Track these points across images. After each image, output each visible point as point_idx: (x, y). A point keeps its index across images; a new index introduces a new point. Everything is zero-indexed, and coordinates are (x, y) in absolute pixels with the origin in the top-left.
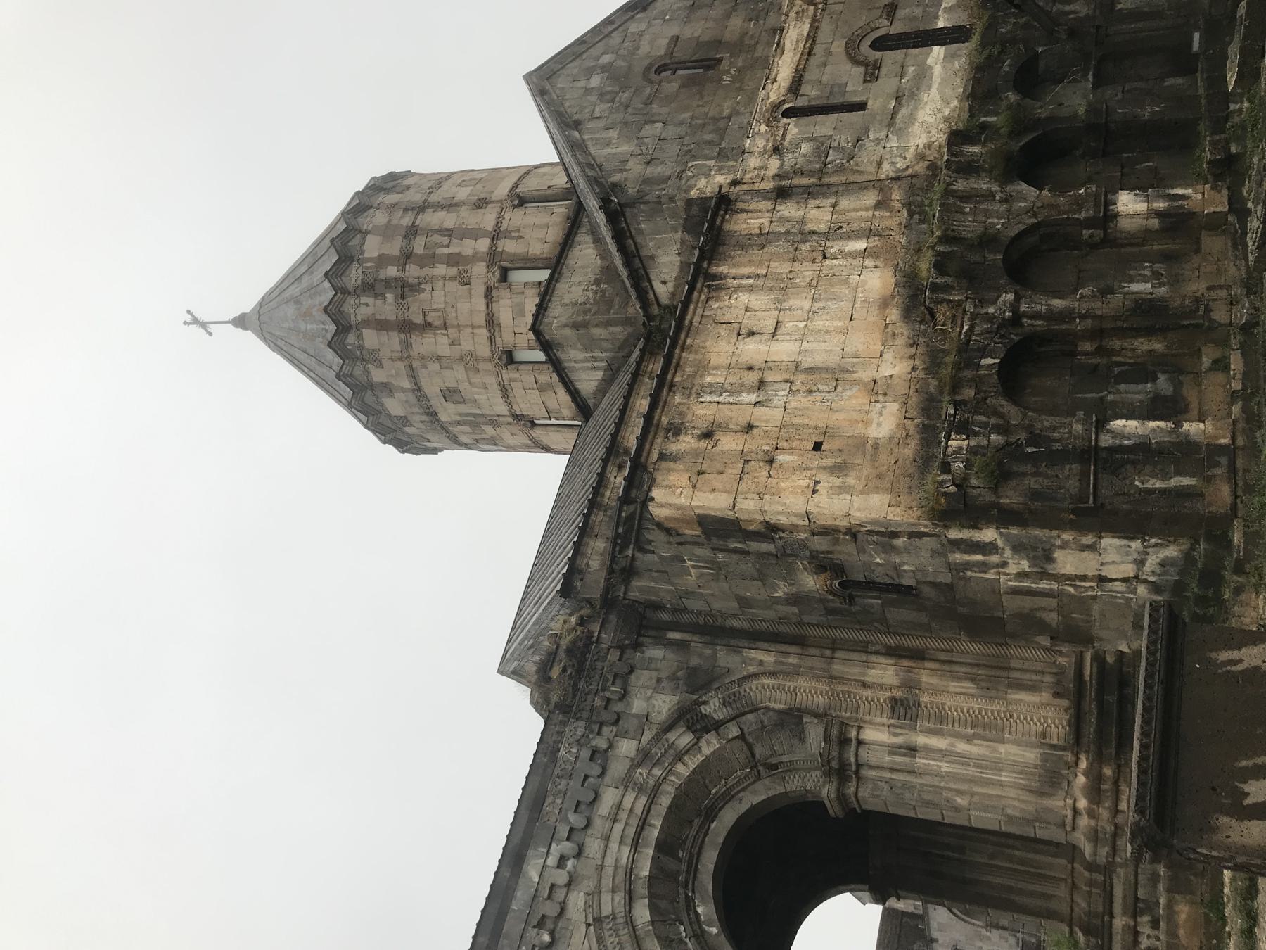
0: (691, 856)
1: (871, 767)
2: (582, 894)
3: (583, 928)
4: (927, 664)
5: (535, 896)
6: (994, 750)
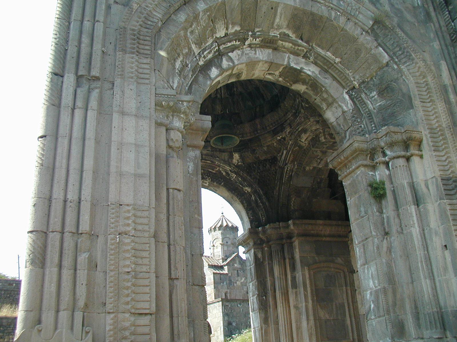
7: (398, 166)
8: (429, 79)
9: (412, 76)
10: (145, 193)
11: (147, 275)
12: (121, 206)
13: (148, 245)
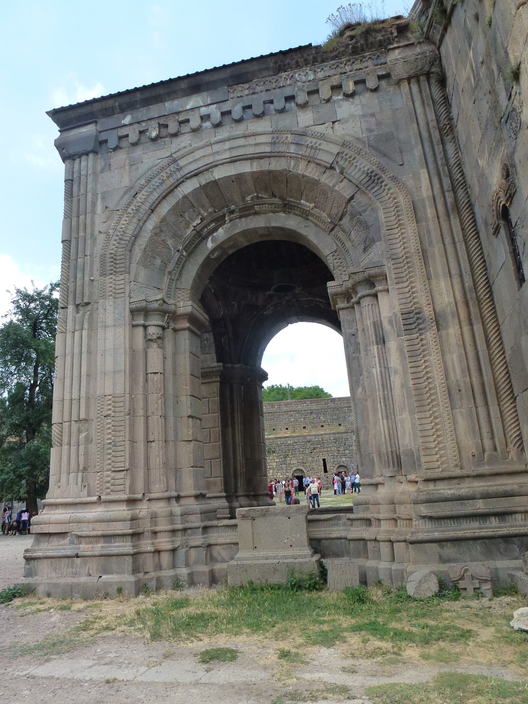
0: (252, 207)
2: (190, 142)
3: (168, 154)
4: (466, 329)
5: (178, 113)
8: (401, 199)
11: (123, 443)
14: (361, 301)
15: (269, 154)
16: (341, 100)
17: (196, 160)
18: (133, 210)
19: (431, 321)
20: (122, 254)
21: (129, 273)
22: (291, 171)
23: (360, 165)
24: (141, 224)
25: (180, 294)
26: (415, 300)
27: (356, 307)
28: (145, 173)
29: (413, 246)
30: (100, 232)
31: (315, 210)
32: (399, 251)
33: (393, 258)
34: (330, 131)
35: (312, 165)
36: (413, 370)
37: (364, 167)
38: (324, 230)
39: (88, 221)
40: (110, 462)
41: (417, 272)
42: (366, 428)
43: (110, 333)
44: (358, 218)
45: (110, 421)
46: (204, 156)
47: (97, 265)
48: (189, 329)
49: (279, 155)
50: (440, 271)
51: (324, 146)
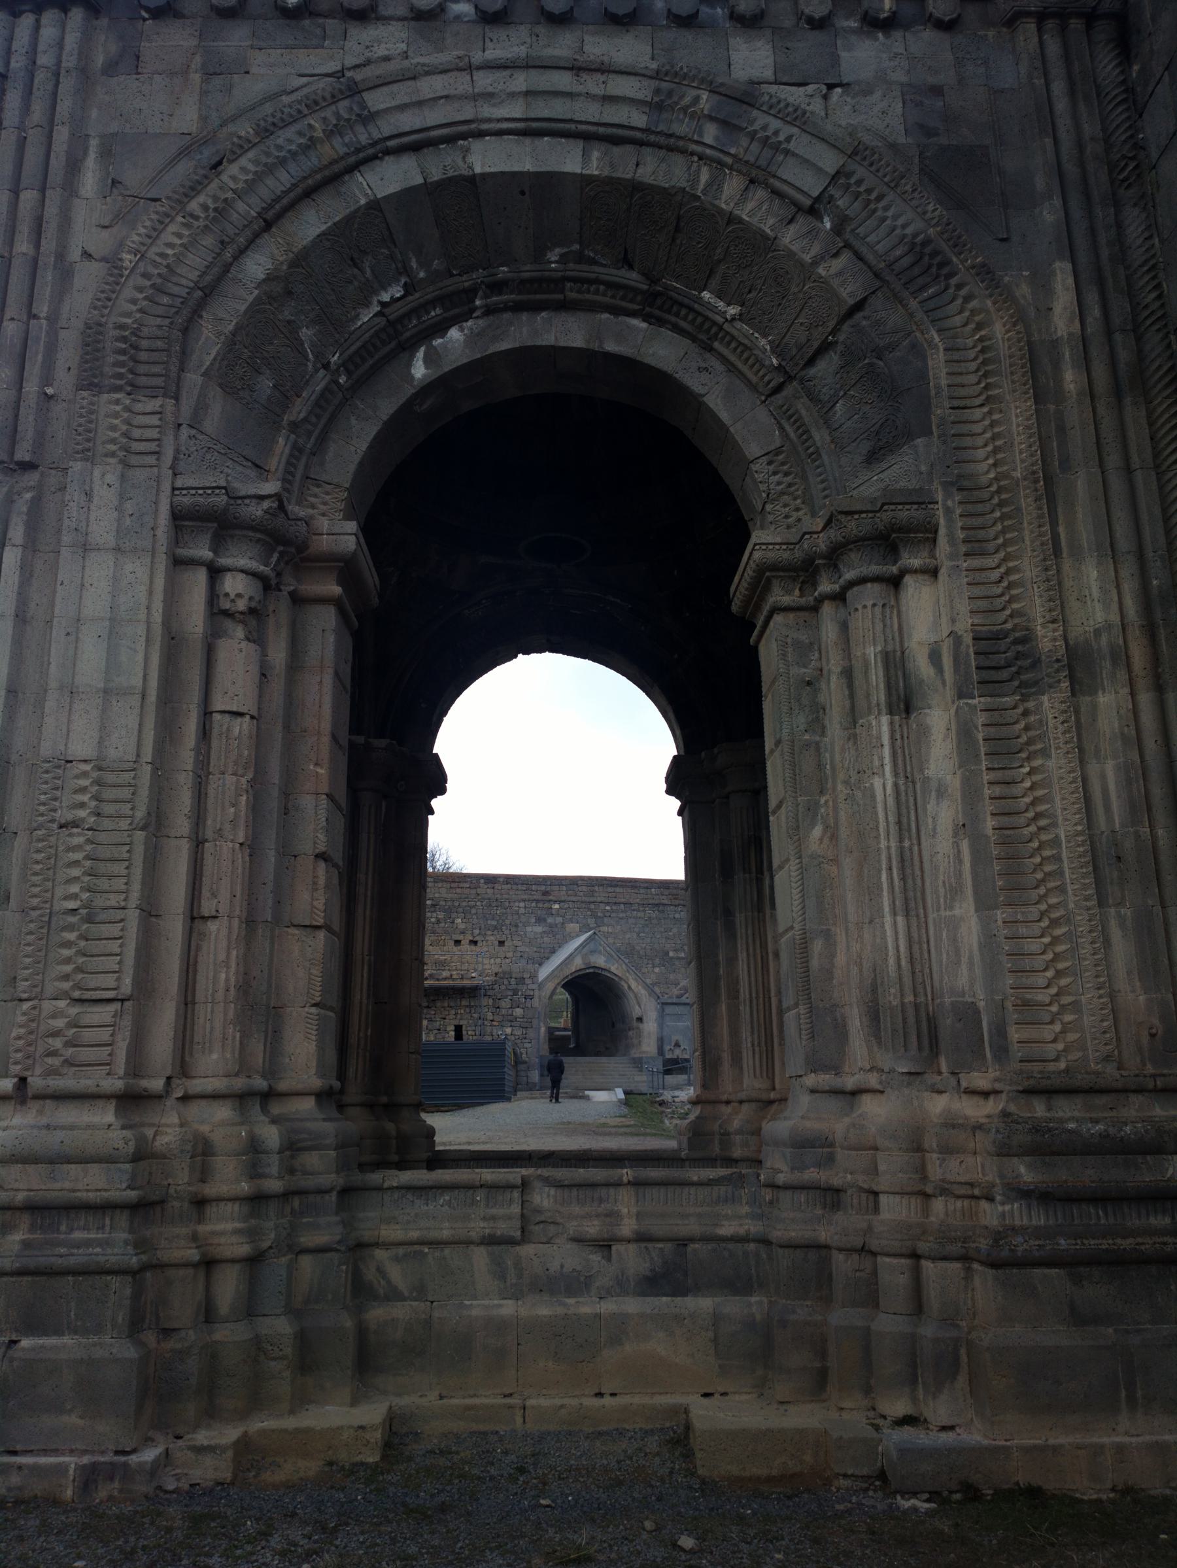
0: (557, 283)
1: (844, 627)
2: (403, 46)
3: (333, 66)
4: (1146, 699)
6: (954, 892)
7: (860, 607)
8: (998, 329)
9: (939, 331)
10: (129, 734)
11: (119, 915)
12: (69, 765)
13: (127, 848)
14: (849, 594)
15: (638, 135)
16: (854, 31)
17: (420, 104)
18: (205, 208)
19: (1056, 666)
20: (159, 333)
21: (177, 399)
22: (698, 198)
23: (895, 217)
24: (228, 255)
25: (316, 496)
26: (1015, 606)
27: (827, 609)
28: (253, 108)
29: (1021, 459)
30: (87, 255)
31: (738, 324)
32: (983, 470)
33: (962, 485)
34: (817, 106)
35: (761, 193)
36: (997, 790)
37: (904, 227)
38: (753, 387)
39: (51, 211)
40: (68, 968)
41: (1027, 532)
42: (828, 936)
43: (100, 570)
44: (871, 365)
45: (77, 840)
46: (446, 97)
47: (68, 355)
48: (337, 602)
49: (671, 146)
50: (1085, 536)
51: (802, 145)
